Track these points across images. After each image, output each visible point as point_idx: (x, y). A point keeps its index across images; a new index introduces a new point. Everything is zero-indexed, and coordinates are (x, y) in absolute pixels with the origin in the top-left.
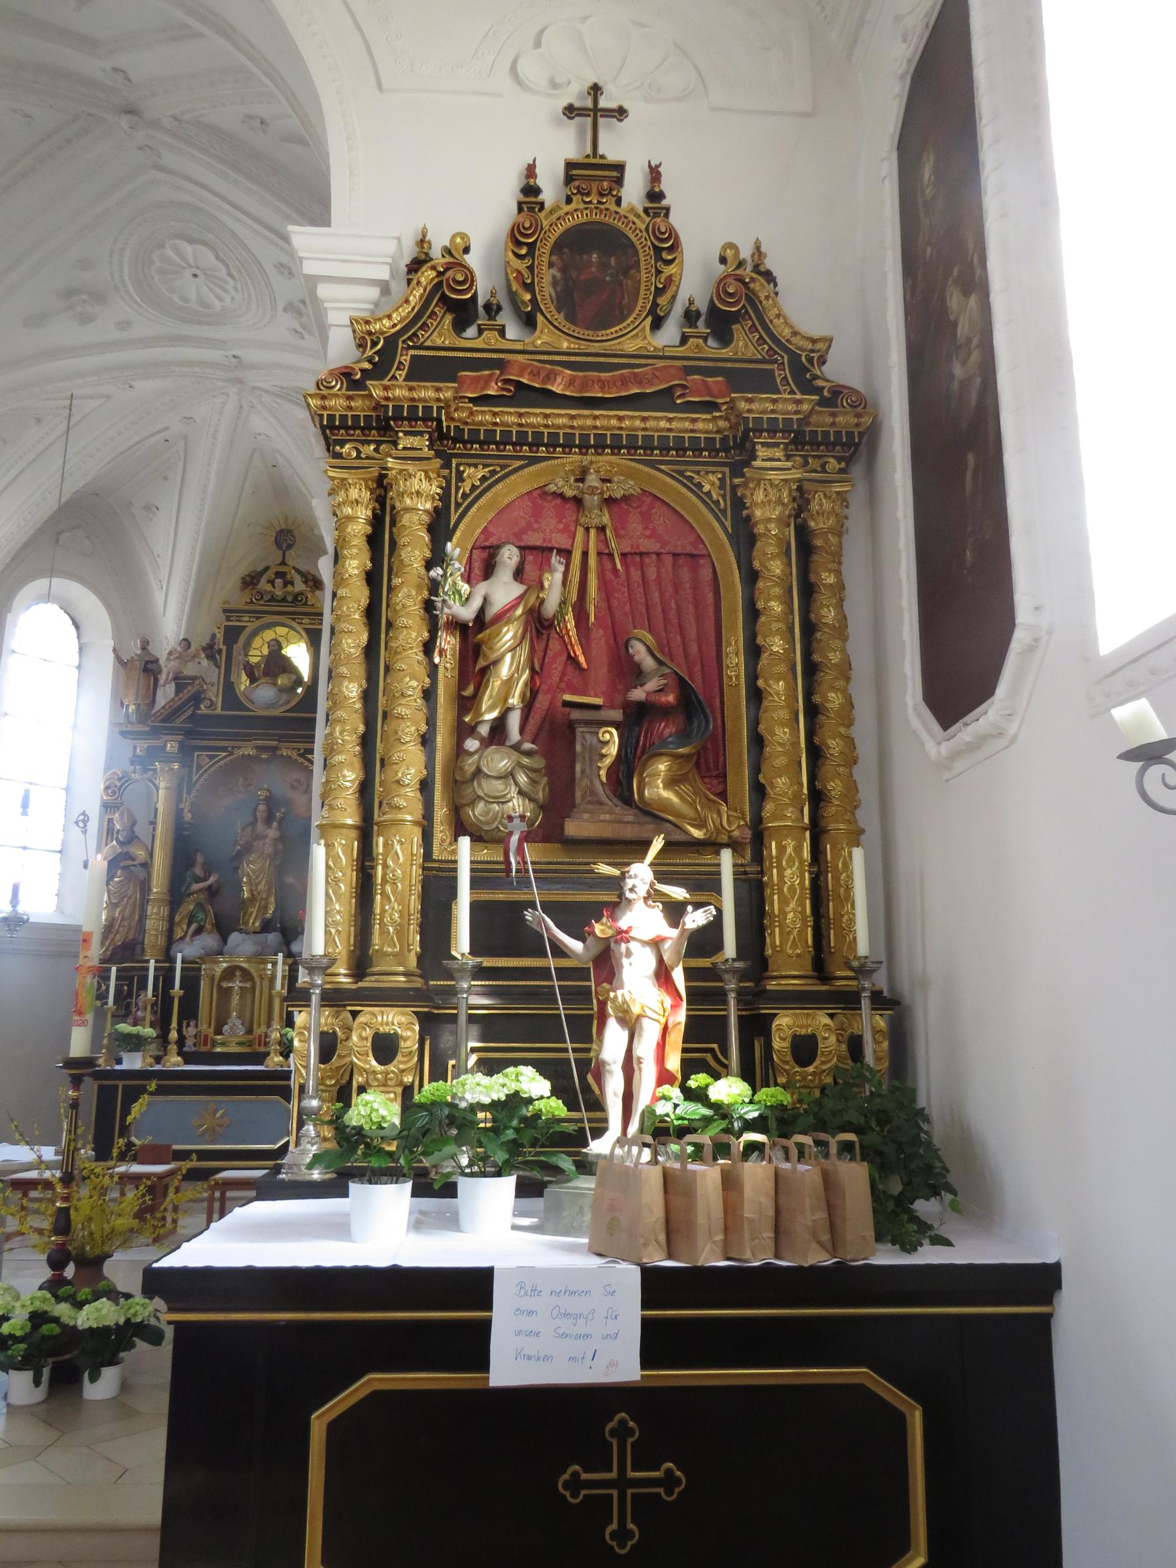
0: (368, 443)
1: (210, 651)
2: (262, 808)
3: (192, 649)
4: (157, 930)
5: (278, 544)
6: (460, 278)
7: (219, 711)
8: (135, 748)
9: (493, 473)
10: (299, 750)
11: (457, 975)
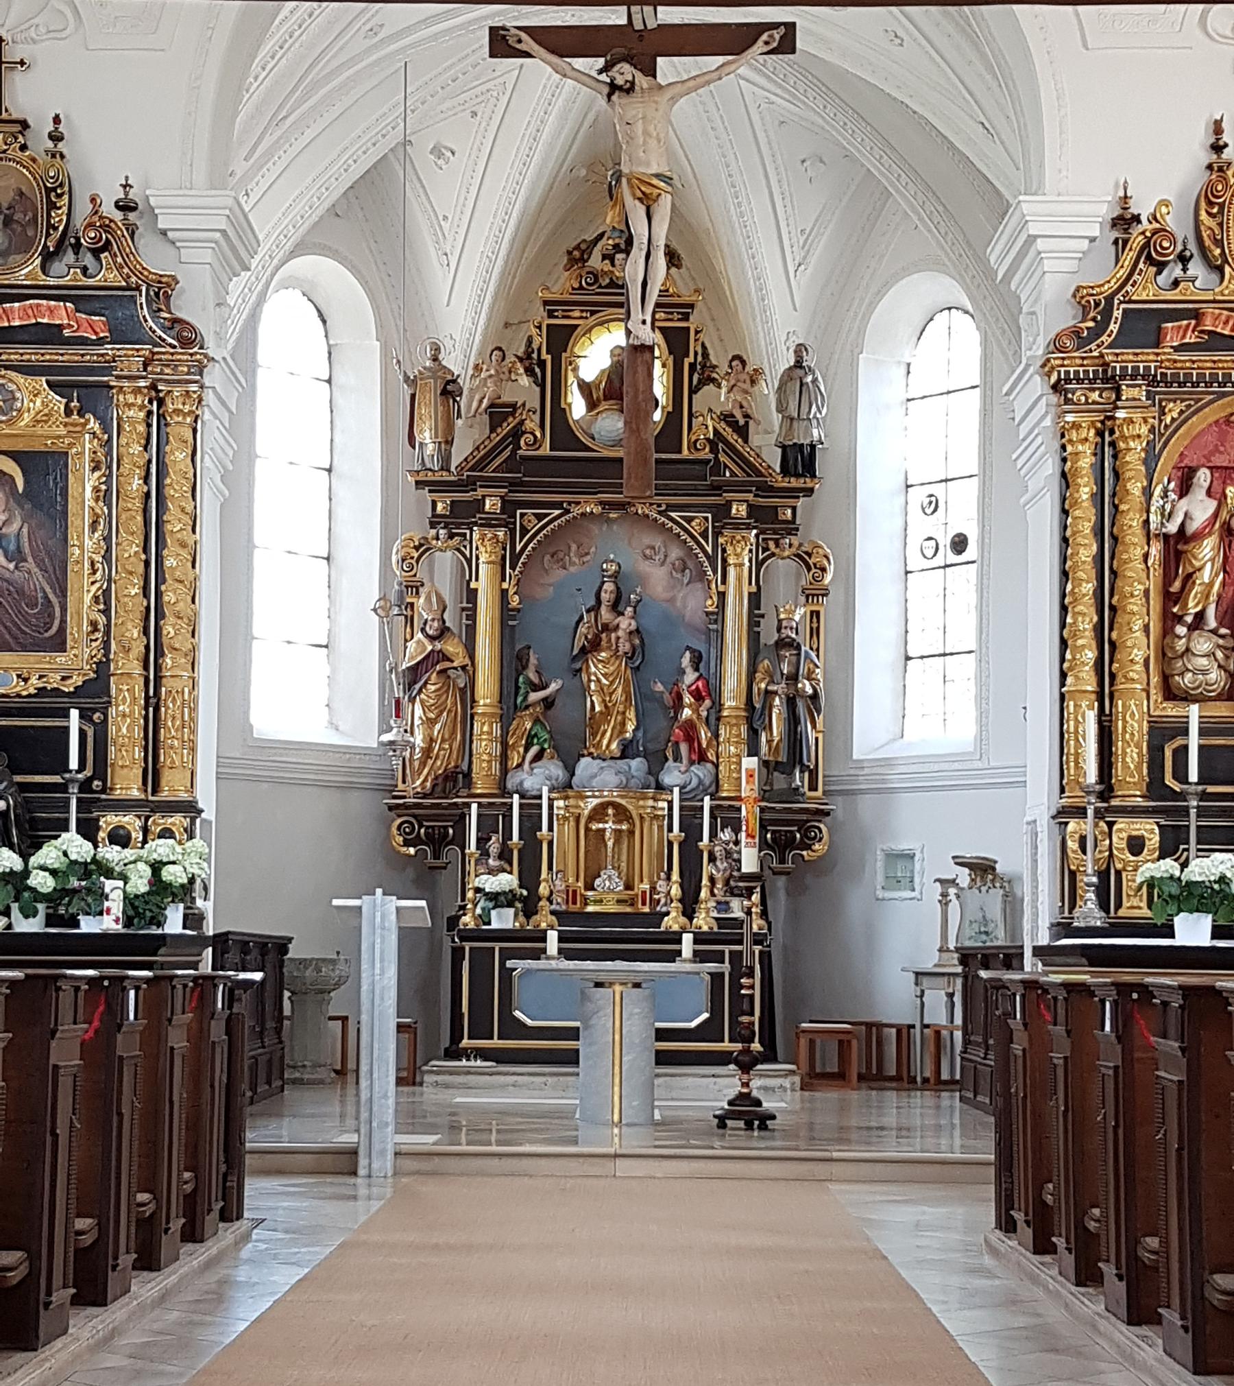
0: (1093, 390)
2: (609, 586)
4: (490, 754)
6: (1166, 244)
7: (546, 450)
8: (434, 503)
9: (1189, 406)
10: (659, 505)
11: (1188, 797)
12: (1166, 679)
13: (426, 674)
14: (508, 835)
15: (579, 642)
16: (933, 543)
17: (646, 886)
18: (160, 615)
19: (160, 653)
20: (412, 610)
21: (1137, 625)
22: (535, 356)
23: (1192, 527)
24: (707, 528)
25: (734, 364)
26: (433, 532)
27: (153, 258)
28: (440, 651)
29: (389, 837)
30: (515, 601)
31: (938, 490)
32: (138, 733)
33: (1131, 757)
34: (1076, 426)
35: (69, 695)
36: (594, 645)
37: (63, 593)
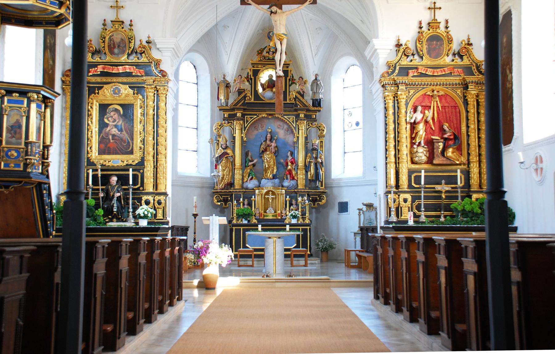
2: (269, 135)
7: (252, 101)
12: (412, 159)
13: (222, 158)
15: (262, 149)
17: (279, 212)
18: (157, 145)
19: (157, 154)
21: (404, 145)
23: (417, 121)
27: (155, 54)
29: (213, 200)
30: (245, 139)
32: (152, 175)
33: (404, 179)
34: (388, 96)
35: (134, 165)
36: (265, 150)
37: (132, 139)
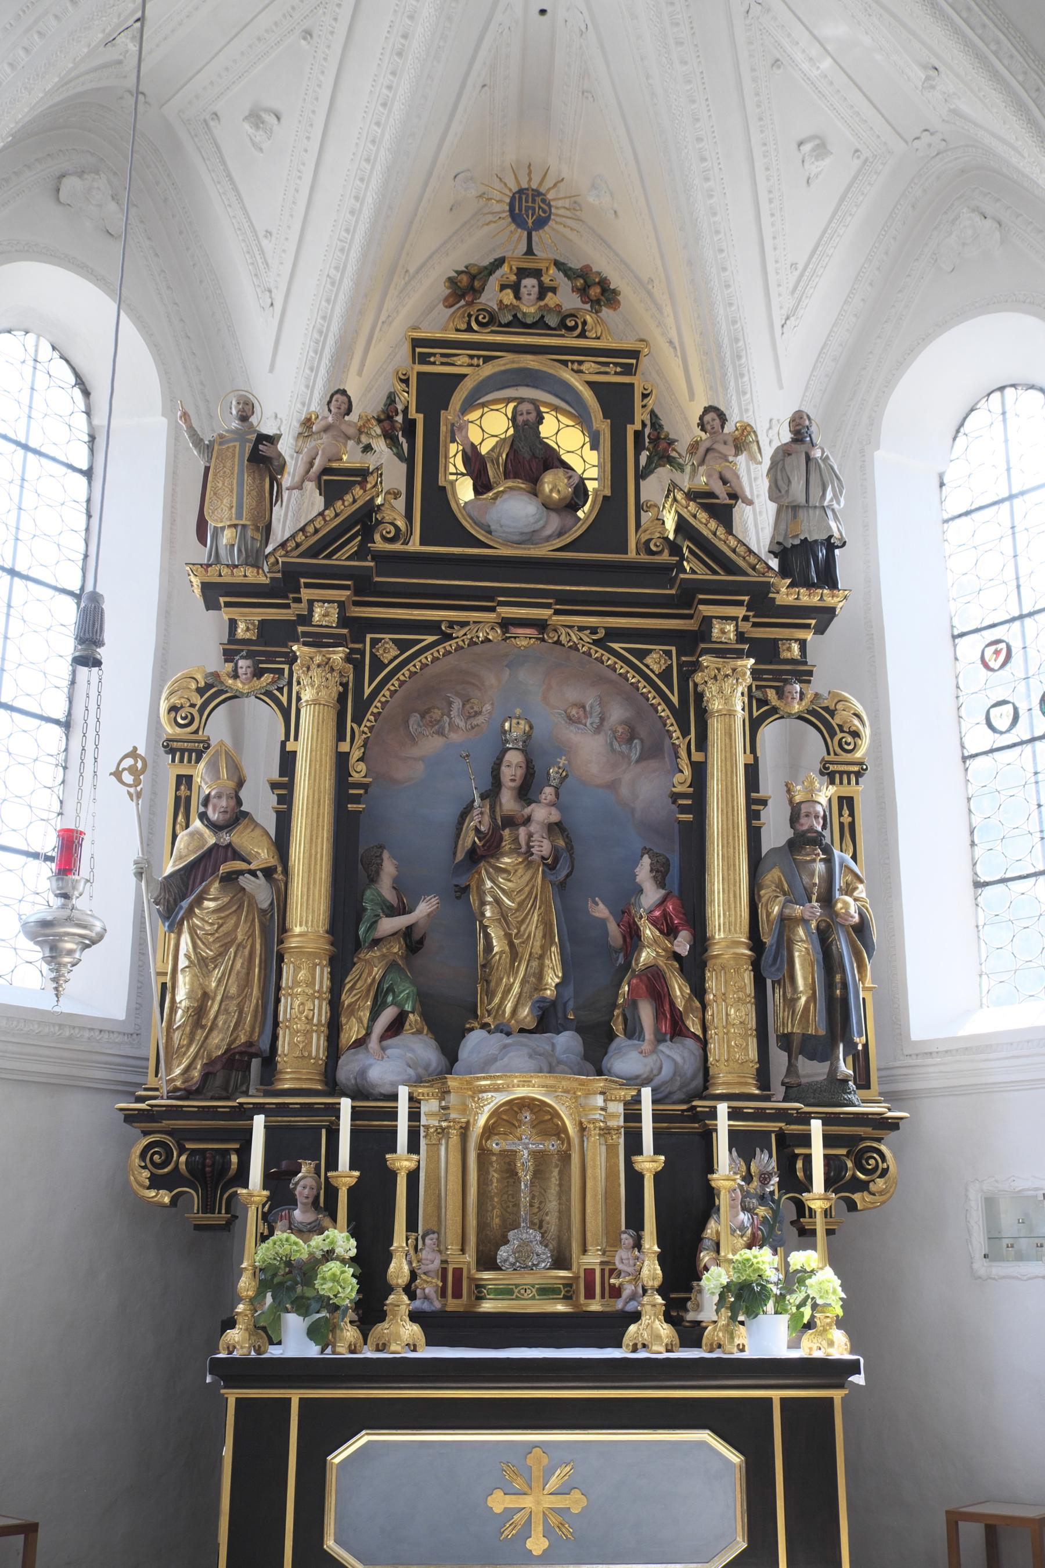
1: (391, 424)
2: (514, 758)
3: (353, 417)
5: (516, 217)
8: (233, 624)
10: (594, 630)
14: (332, 1163)
16: (1009, 708)
20: (189, 787)
22: (399, 418)
24: (671, 666)
25: (707, 418)
26: (229, 666)
28: (230, 845)
30: (358, 772)
31: (1011, 634)
36: (485, 852)
